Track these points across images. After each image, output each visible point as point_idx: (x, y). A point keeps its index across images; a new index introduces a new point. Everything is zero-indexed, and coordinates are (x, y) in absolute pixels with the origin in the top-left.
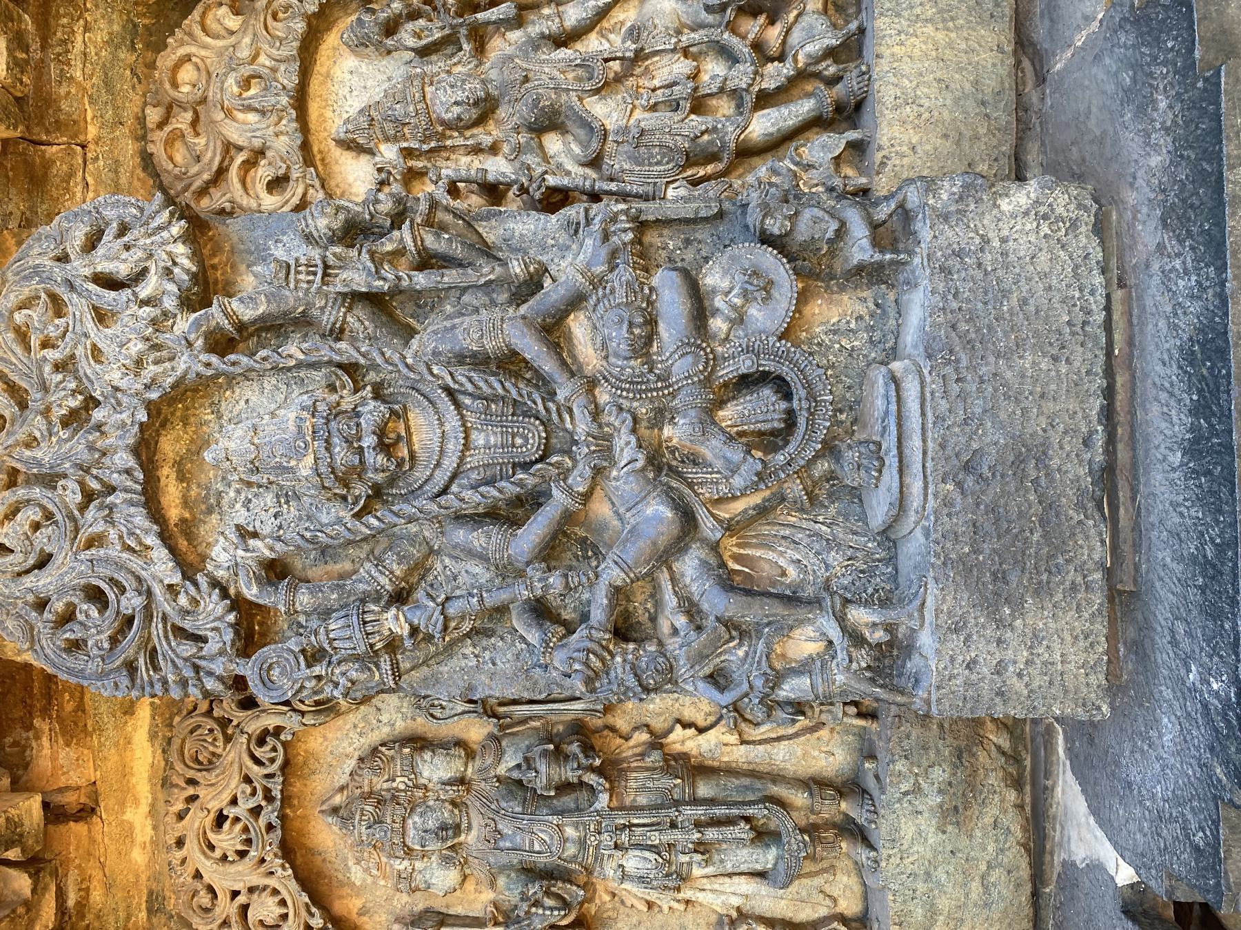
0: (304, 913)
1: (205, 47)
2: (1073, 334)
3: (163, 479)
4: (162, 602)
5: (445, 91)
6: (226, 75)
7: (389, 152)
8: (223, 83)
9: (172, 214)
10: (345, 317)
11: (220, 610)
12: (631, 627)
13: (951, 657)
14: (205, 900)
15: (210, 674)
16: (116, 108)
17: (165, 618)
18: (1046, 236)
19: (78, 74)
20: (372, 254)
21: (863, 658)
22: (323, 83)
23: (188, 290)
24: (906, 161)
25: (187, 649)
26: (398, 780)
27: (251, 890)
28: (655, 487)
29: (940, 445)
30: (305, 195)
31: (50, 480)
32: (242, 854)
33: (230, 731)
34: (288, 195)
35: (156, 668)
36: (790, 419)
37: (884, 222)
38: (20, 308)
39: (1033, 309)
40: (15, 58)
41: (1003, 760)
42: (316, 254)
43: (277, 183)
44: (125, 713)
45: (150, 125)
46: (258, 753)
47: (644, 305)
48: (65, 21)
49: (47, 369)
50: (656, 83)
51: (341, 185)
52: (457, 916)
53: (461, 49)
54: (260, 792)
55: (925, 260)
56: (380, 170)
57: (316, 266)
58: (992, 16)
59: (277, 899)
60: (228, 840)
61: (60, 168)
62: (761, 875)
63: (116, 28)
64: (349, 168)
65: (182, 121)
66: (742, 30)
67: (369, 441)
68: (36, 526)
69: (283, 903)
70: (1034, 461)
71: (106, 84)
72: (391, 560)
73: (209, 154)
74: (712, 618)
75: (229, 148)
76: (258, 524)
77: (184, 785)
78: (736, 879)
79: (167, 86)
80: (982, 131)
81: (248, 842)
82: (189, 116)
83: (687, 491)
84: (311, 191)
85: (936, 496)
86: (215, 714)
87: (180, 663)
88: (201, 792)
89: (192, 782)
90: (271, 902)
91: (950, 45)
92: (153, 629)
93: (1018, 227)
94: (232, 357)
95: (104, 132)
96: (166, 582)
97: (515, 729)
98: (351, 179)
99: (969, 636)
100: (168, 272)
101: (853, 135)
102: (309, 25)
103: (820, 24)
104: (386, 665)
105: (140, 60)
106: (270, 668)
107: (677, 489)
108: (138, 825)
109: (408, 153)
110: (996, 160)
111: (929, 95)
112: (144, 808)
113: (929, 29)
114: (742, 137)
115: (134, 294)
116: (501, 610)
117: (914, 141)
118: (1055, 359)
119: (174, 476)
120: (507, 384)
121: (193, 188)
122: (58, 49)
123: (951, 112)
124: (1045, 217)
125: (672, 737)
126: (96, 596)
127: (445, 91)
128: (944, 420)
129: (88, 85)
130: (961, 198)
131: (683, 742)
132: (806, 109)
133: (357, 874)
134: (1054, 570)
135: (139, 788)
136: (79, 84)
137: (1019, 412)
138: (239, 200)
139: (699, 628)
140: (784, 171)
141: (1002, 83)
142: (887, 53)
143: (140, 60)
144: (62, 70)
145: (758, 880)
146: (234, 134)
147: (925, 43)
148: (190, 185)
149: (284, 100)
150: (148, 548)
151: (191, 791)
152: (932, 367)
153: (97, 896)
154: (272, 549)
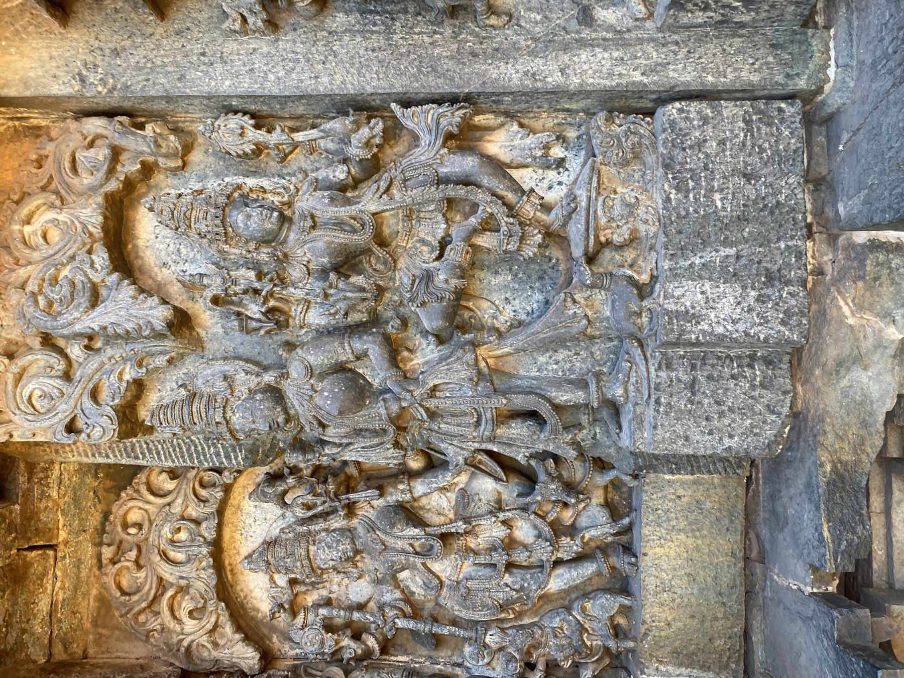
1: (148, 502)
5: (324, 551)
6: (162, 525)
8: (160, 532)
16: (81, 520)
19: (55, 494)
22: (235, 513)
24: (663, 633)
30: (216, 622)
45: (104, 561)
51: (245, 590)
58: (728, 529)
61: (37, 568)
64: (251, 578)
71: (75, 501)
73: (147, 588)
79: (119, 529)
80: (720, 615)
82: (133, 554)
91: (697, 549)
95: (71, 538)
98: (252, 586)
103: (602, 516)
105: (101, 486)
110: (730, 638)
111: (680, 584)
113: (682, 536)
117: (669, 619)
122: (41, 475)
123: (696, 598)
127: (324, 551)
129: (61, 502)
132: (590, 572)
136: (55, 501)
138: (167, 624)
140: (573, 624)
141: (735, 580)
142: (650, 553)
143: (101, 486)
144: (43, 491)
146: (167, 572)
147: (679, 546)
148: (131, 610)
149: (205, 550)
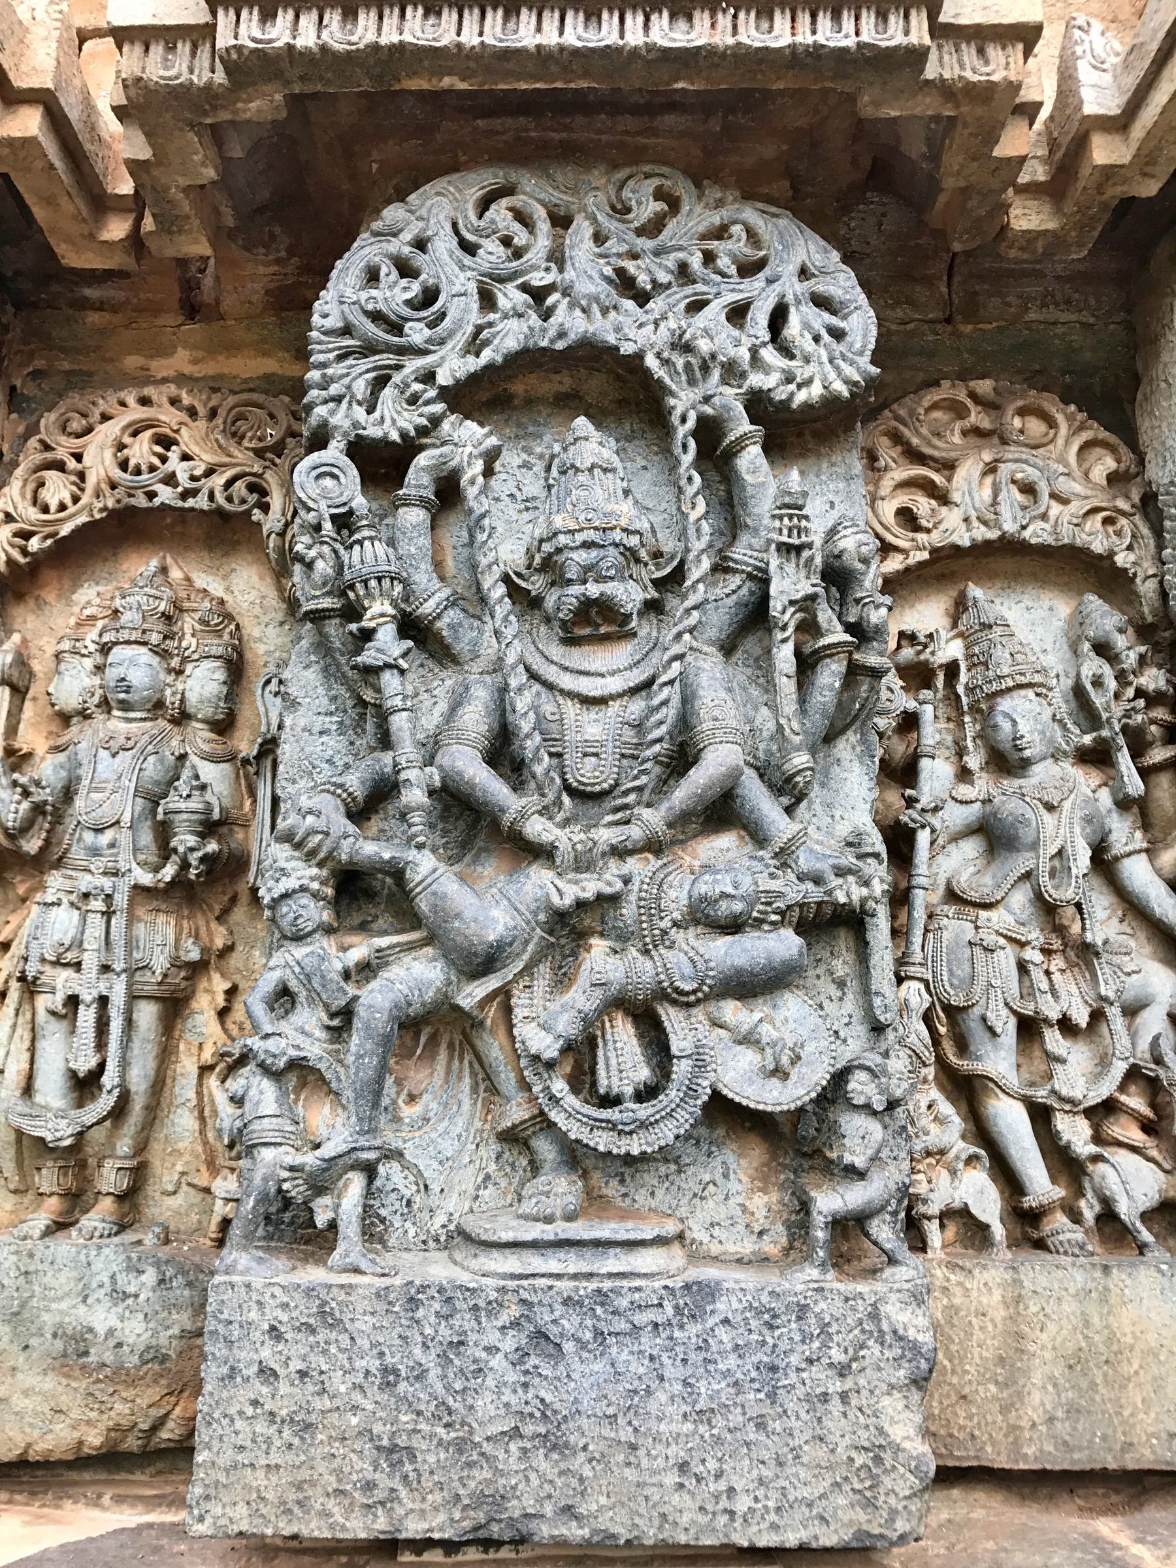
0: (48, 530)
1: (1067, 443)
2: (717, 1497)
3: (558, 377)
4: (413, 365)
7: (951, 650)
9: (856, 384)
10: (743, 571)
11: (402, 423)
12: (354, 898)
13: (287, 1305)
14: (76, 425)
15: (332, 412)
17: (398, 368)
18: (851, 1460)
20: (813, 598)
21: (296, 1189)
23: (770, 400)
25: (361, 388)
26: (194, 641)
27: (82, 476)
28: (528, 923)
29: (569, 1298)
31: (557, 258)
32: (124, 465)
33: (269, 455)
34: (897, 530)
35: (341, 358)
36: (610, 1101)
37: (867, 1235)
38: (748, 232)
39: (752, 1436)
40: (1036, 238)
41: (145, 1426)
42: (817, 539)
43: (907, 517)
45: (972, 384)
46: (240, 485)
47: (755, 914)
48: (1092, 302)
49: (681, 255)
50: (1057, 977)
52: (21, 710)
53: (1084, 732)
55: (816, 1285)
56: (931, 636)
57: (799, 537)
59: (68, 501)
60: (141, 450)
61: (920, 293)
63: (1088, 356)
65: (977, 417)
66: (1133, 1088)
67: (593, 590)
68: (507, 241)
69: (62, 507)
70: (543, 1431)
72: (453, 615)
74: (357, 992)
75: (948, 467)
76: (503, 476)
77: (211, 404)
78: (26, 1056)
79: (1020, 403)
81: (138, 472)
82: (986, 424)
83: (520, 965)
84: (901, 557)
85: (502, 1290)
86: (288, 440)
87: (347, 380)
89: (213, 414)
92: (385, 356)
93: (862, 1419)
94: (692, 444)
96: (439, 370)
97: (243, 782)
99: (313, 1331)
100: (789, 379)
101: (998, 1231)
102: (1100, 556)
104: (327, 603)
106: (334, 476)
107: (524, 951)
109: (952, 669)
110: (973, 1436)
112: (188, 369)
114: (991, 1085)
115: (764, 344)
116: (385, 741)
118: (683, 1467)
119: (562, 389)
120: (657, 748)
121: (902, 428)
124: (878, 1460)
125: (216, 977)
126: (430, 296)
128: (602, 1304)
130: (901, 1338)
134: (396, 1456)
137: (611, 1411)
139: (346, 975)
144: (1035, 299)
145: (23, 1084)
148: (905, 425)
150: (477, 355)
151: (202, 411)
152: (673, 1289)
153: (94, 318)
154: (472, 482)
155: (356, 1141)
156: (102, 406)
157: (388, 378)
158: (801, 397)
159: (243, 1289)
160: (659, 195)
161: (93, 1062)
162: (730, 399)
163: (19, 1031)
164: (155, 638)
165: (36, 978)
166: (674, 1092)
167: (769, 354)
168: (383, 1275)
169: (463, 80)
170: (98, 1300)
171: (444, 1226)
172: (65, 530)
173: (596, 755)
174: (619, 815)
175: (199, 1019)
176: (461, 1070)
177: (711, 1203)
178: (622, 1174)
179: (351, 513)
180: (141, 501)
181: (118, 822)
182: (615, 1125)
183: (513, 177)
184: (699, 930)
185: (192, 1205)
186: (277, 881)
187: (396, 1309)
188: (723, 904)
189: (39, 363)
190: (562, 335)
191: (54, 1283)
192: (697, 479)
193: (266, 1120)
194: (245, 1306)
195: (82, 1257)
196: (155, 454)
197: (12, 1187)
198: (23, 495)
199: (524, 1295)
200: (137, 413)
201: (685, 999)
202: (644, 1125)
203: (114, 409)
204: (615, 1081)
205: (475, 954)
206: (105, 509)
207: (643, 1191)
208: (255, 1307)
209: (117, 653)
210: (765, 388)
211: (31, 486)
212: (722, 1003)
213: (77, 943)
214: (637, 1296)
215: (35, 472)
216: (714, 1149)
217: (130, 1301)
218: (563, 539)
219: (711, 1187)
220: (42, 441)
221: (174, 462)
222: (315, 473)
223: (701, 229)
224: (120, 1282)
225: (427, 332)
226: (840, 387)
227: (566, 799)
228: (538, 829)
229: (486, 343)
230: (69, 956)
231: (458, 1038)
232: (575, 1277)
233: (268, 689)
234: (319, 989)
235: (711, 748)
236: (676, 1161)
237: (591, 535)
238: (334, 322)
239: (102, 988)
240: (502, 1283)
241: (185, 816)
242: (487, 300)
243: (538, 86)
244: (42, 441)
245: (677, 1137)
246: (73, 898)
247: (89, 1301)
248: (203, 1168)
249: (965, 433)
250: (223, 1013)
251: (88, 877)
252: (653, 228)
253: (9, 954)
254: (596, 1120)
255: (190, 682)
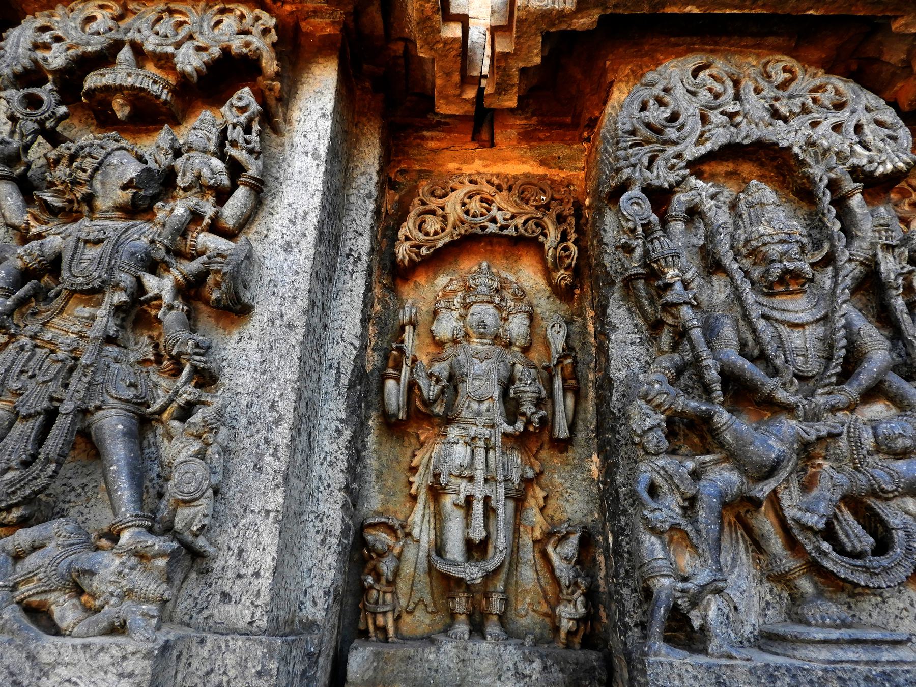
0: (429, 244)
4: (671, 150)
14: (439, 192)
17: (662, 151)
25: (645, 161)
31: (737, 97)
32: (467, 212)
44: (541, 161)
54: (507, 223)
60: (475, 205)
62: (439, 549)
68: (710, 90)
69: (436, 233)
85: (825, 670)
88: (505, 193)
90: (438, 227)
94: (828, 192)
106: (638, 204)
108: (471, 166)
112: (482, 170)
119: (729, 169)
125: (538, 489)
126: (674, 117)
131: (534, 497)
133: (442, 281)
135: (495, 167)
151: (505, 186)
155: (715, 575)
156: (452, 184)
157: (657, 156)
158: (881, 170)
159: (668, 666)
160: (785, 70)
161: (484, 534)
162: (840, 171)
163: (427, 518)
164: (497, 300)
165: (447, 485)
166: (899, 550)
167: (858, 148)
168: (748, 660)
169: (697, 8)
170: (508, 679)
171: (751, 632)
172: (440, 245)
173: (802, 355)
174: (827, 389)
175: (530, 513)
176: (737, 538)
177: (907, 622)
178: (849, 603)
179: (650, 223)
180: (480, 231)
181: (491, 397)
182: (868, 569)
183: (711, 59)
184: (881, 456)
185: (536, 624)
186: (644, 420)
187: (763, 681)
188: (900, 441)
189: (404, 166)
190: (747, 136)
191: (482, 667)
192: (833, 210)
193: (659, 561)
194: (671, 677)
195: (496, 651)
196: (482, 207)
197: (430, 609)
198: (415, 227)
199: (840, 674)
200: (472, 187)
201: (886, 496)
202: (887, 570)
203: (458, 186)
204: (858, 545)
205: (765, 466)
206: (460, 234)
207: (864, 613)
208: (677, 678)
209: (475, 308)
210: (861, 165)
211: (418, 223)
212: (905, 499)
213: (472, 464)
214: (908, 676)
215: (419, 215)
216: (902, 588)
217: (527, 680)
218: (767, 239)
219: (905, 612)
220: (421, 200)
221: (494, 212)
222: (630, 202)
223: (811, 87)
224: (520, 668)
225: (678, 134)
226: (901, 165)
227: (796, 380)
228: (782, 395)
229: (707, 140)
230: (466, 473)
231: (733, 519)
232: (867, 663)
233: (553, 330)
234: (679, 484)
235: (873, 352)
236: (881, 595)
237: (783, 236)
238: (628, 127)
239: (487, 491)
240: (824, 666)
241: (530, 395)
242: (704, 119)
243: (735, 11)
244: (421, 200)
245: (907, 577)
246: (467, 439)
247: (502, 679)
248: (543, 601)
249: (910, 205)
250: (542, 510)
251: (475, 428)
252: (783, 86)
253: (418, 474)
254: (854, 566)
255: (512, 326)
